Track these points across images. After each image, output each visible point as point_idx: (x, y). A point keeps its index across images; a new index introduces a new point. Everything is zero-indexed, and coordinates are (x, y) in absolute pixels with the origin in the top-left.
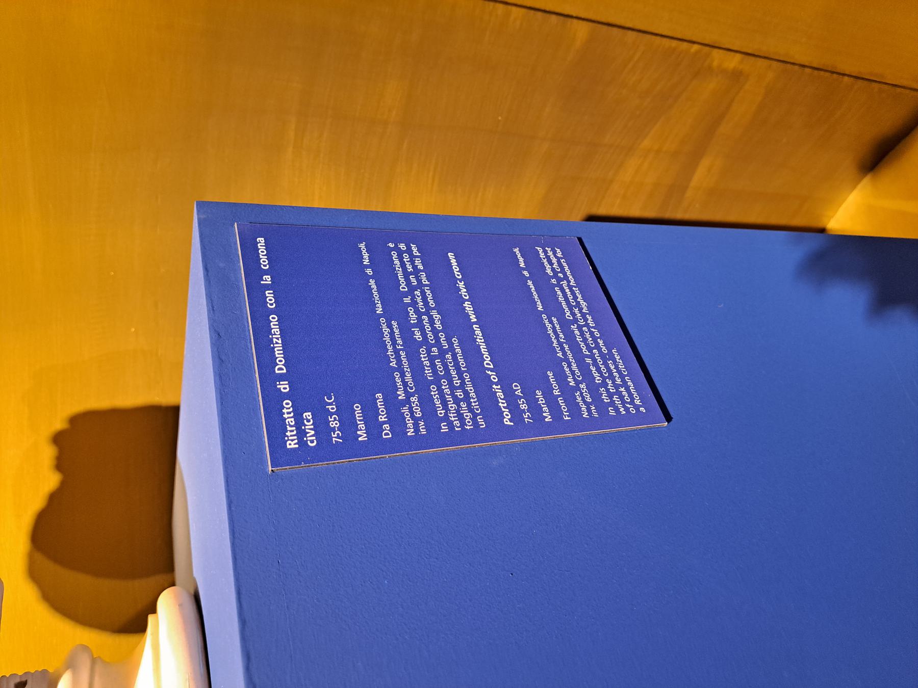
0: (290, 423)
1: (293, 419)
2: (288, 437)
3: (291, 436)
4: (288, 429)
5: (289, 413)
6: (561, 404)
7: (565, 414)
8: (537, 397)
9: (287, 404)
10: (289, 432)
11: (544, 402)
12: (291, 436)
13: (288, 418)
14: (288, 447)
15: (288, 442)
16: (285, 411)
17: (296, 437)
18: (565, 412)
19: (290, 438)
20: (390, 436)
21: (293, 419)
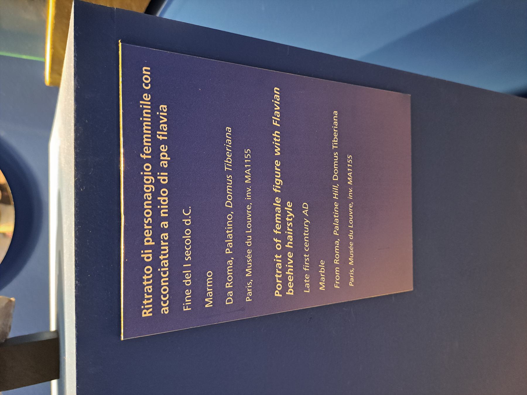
0: (148, 290)
1: (151, 287)
9: (148, 270)
11: (324, 272)
16: (145, 277)
21: (151, 287)
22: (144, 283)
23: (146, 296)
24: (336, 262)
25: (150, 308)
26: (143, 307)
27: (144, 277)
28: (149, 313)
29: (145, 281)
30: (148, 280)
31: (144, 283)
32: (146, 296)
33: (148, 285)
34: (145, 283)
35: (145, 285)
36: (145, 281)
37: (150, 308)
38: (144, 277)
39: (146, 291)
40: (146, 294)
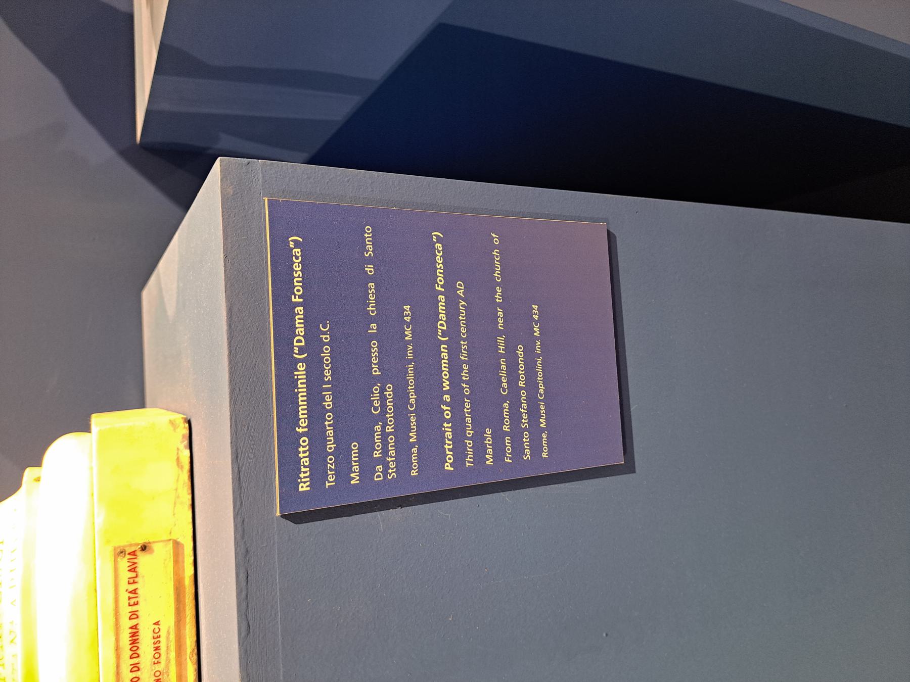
0: (305, 462)
2: (301, 479)
3: (305, 477)
4: (302, 470)
5: (304, 452)
6: (507, 444)
7: (508, 455)
8: (485, 435)
10: (302, 473)
12: (305, 477)
13: (304, 457)
14: (301, 489)
15: (301, 485)
16: (301, 449)
17: (308, 479)
18: (508, 454)
19: (303, 480)
20: (382, 479)
22: (300, 455)
23: (303, 469)
24: (506, 428)
25: (307, 482)
26: (299, 480)
27: (300, 449)
28: (307, 487)
29: (302, 453)
30: (304, 452)
31: (300, 455)
32: (303, 469)
33: (304, 457)
34: (301, 455)
35: (302, 457)
36: (302, 453)
37: (307, 482)
38: (300, 449)
39: (302, 464)
40: (302, 467)
